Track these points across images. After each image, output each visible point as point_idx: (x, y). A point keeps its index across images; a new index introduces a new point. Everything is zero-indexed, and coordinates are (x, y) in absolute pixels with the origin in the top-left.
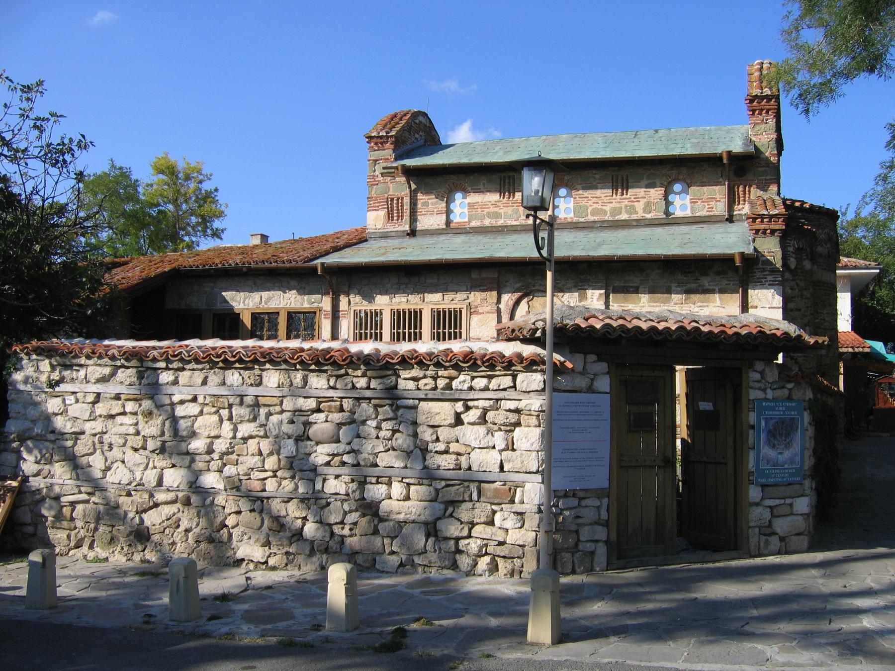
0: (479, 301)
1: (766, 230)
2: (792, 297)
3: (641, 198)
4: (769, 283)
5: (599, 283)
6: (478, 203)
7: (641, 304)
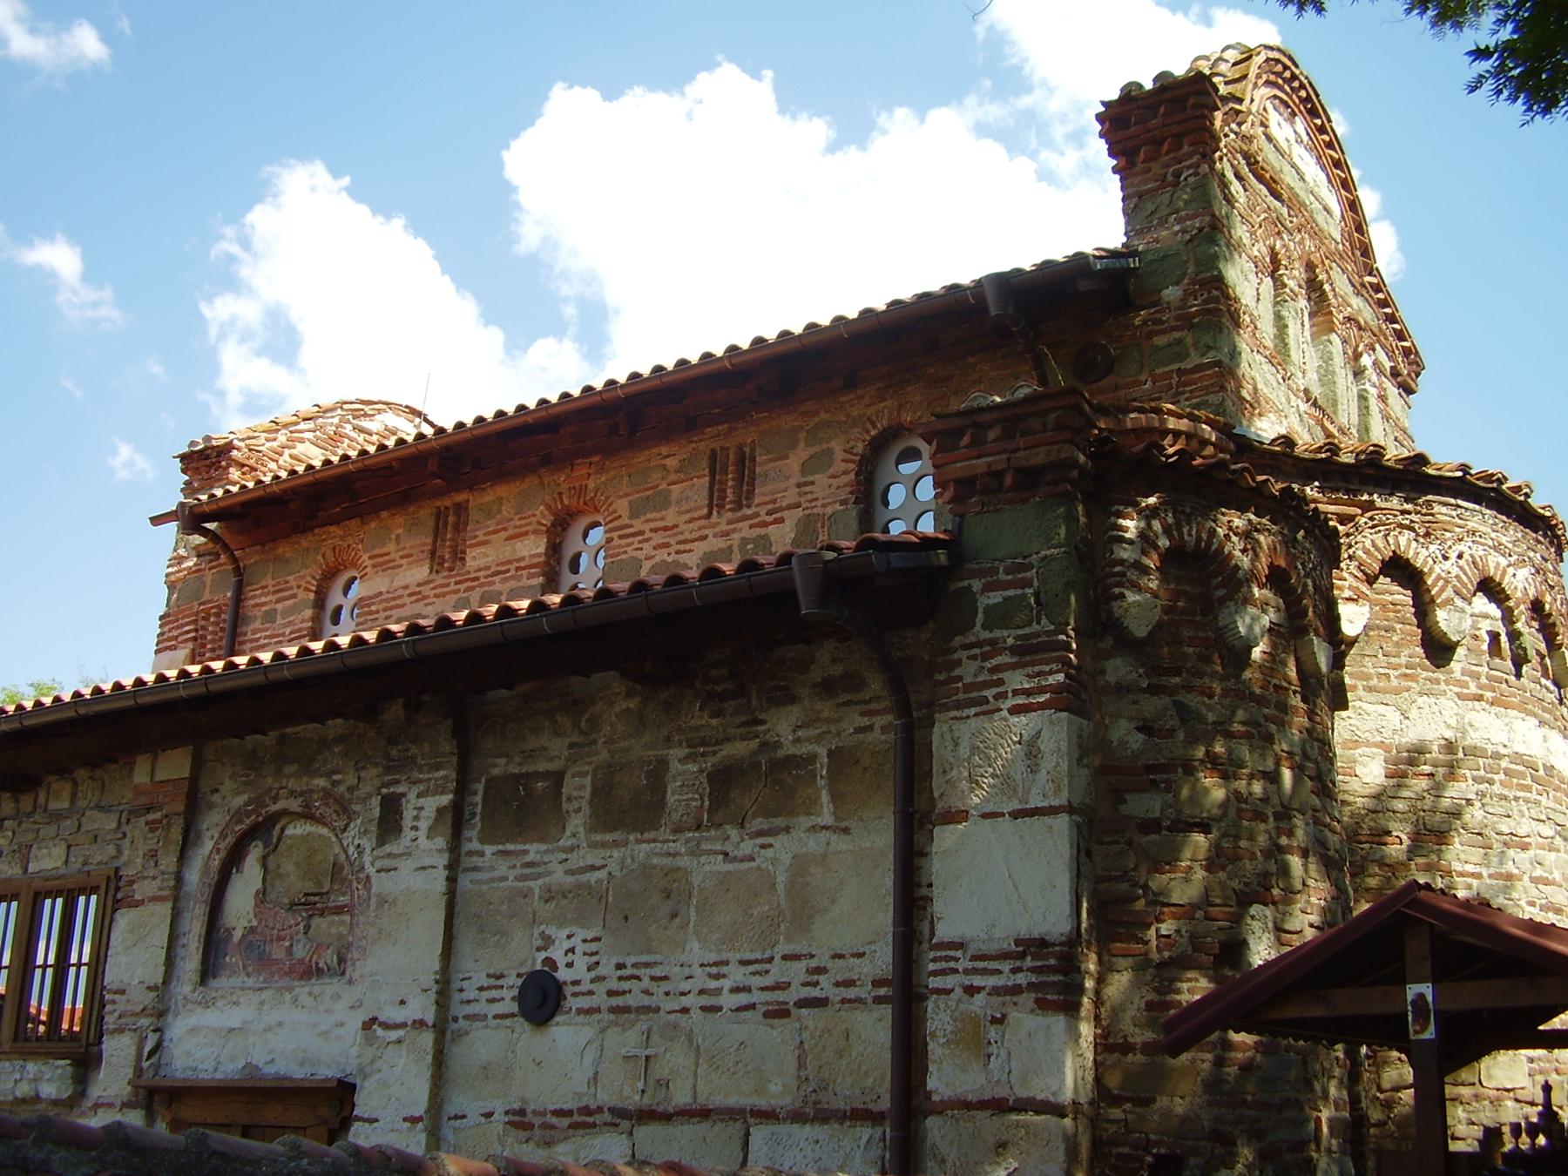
0: (139, 860)
1: (999, 475)
2: (1149, 769)
3: (789, 507)
4: (1010, 702)
5: (438, 767)
6: (381, 593)
7: (565, 842)
